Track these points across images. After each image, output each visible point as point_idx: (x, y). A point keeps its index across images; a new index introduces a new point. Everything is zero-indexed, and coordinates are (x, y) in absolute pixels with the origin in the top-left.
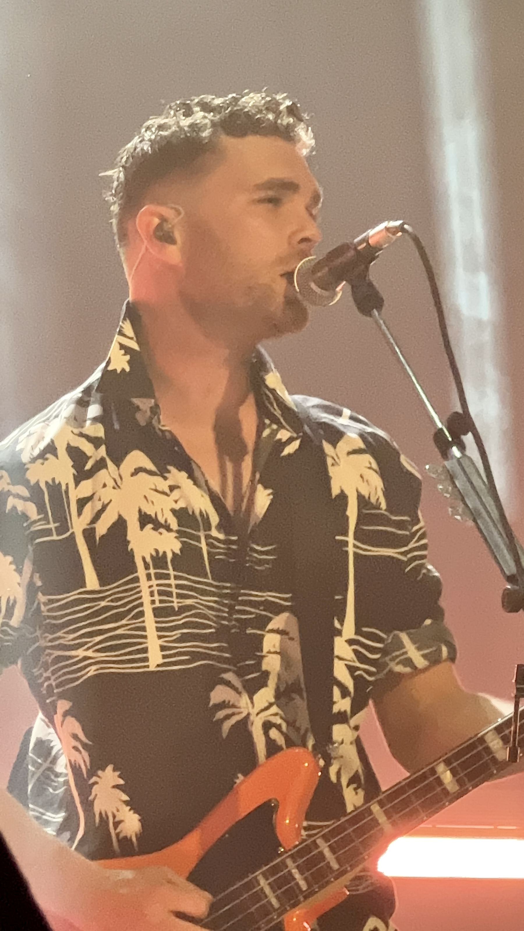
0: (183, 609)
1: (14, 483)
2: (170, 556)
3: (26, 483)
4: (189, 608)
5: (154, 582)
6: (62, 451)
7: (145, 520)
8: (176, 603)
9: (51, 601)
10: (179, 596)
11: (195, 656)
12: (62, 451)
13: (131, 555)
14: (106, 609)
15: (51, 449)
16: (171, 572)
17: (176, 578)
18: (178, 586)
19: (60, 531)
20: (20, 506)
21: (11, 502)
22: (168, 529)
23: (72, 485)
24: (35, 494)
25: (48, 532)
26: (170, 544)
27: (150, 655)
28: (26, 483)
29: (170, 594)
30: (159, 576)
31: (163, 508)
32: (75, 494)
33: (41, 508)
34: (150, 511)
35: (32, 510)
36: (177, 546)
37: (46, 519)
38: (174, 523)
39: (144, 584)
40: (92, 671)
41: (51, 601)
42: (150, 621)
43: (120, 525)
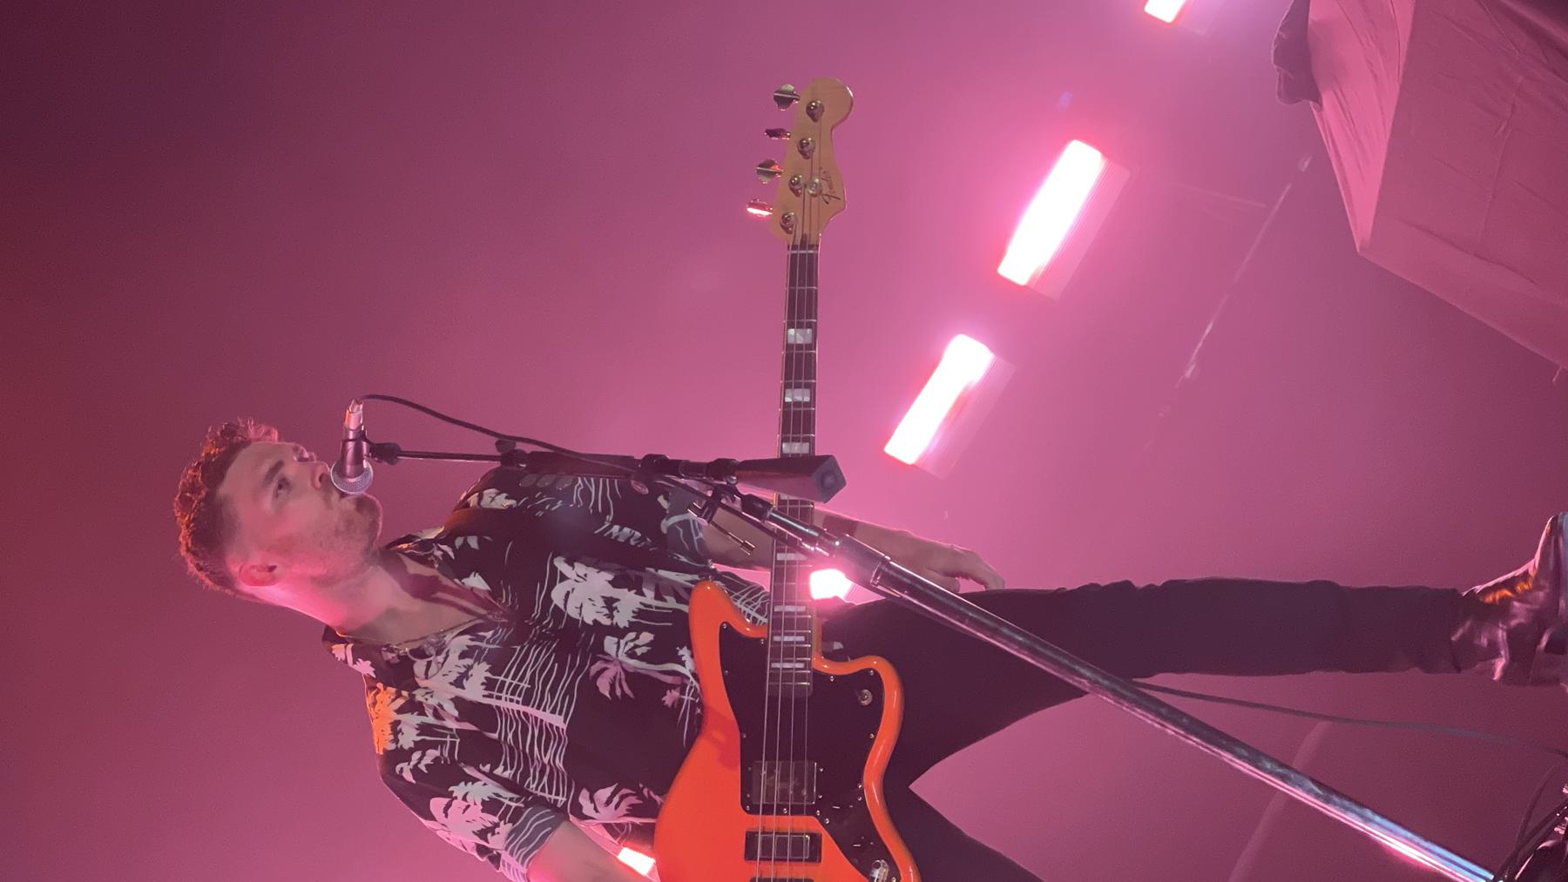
0: (532, 681)
1: (409, 760)
3: (412, 751)
4: (533, 674)
5: (503, 695)
7: (458, 683)
8: (525, 685)
10: (521, 680)
11: (569, 691)
20: (427, 760)
22: (470, 668)
23: (423, 719)
24: (421, 746)
26: (481, 671)
27: (555, 724)
28: (412, 751)
30: (500, 690)
31: (455, 665)
35: (432, 754)
38: (469, 661)
39: (503, 704)
40: (559, 764)
43: (458, 701)
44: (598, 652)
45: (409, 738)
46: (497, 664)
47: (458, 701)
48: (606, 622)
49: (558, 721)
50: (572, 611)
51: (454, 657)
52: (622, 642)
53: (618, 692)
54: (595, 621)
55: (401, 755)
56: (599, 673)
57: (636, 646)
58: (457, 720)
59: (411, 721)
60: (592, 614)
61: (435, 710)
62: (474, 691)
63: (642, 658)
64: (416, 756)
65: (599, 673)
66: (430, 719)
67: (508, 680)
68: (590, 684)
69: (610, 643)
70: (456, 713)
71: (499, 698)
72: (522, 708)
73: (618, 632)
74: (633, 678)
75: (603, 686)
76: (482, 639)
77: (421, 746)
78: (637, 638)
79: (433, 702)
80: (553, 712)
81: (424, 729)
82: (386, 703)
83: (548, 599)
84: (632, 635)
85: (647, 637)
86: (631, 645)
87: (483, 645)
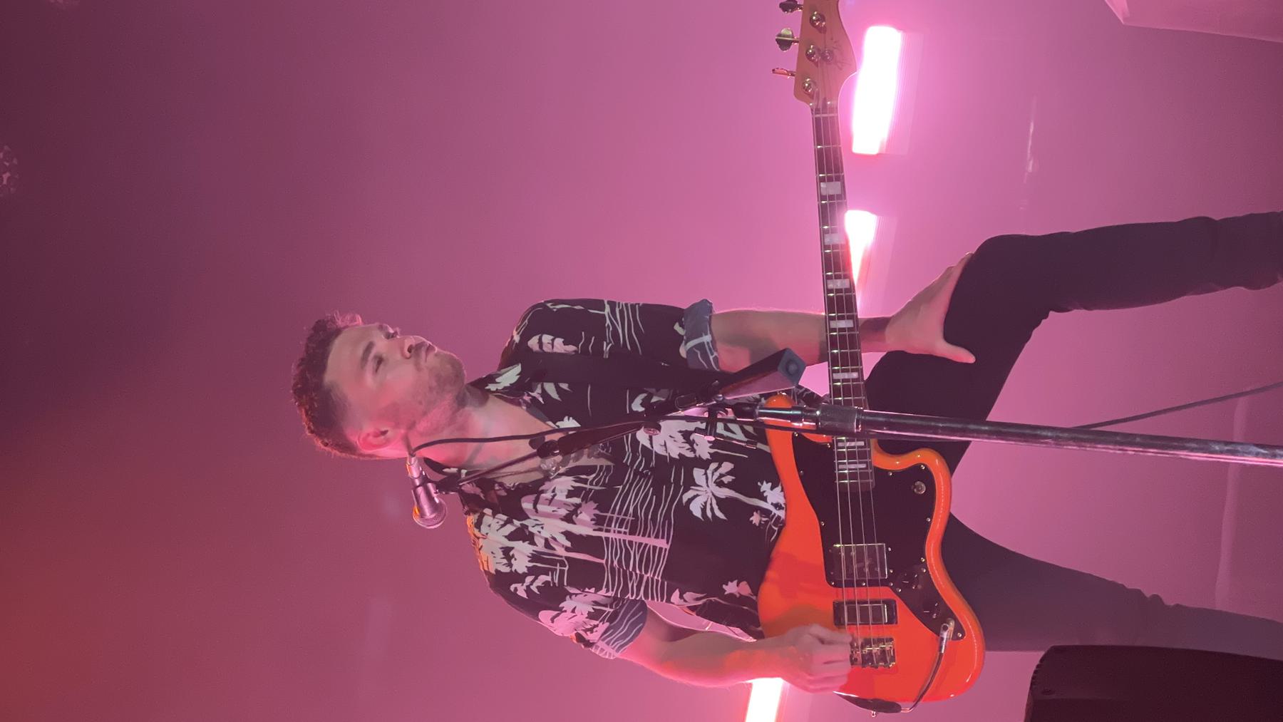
1: (523, 582)
2: (597, 512)
4: (635, 508)
6: (511, 544)
8: (630, 518)
9: (607, 586)
10: (626, 514)
11: (667, 516)
12: (511, 544)
13: (589, 537)
14: (620, 562)
15: (507, 552)
16: (609, 514)
17: (613, 512)
18: (619, 513)
19: (563, 564)
21: (534, 588)
23: (535, 548)
25: (562, 572)
28: (525, 575)
29: (623, 520)
30: (609, 525)
32: (540, 546)
33: (546, 572)
34: (563, 512)
36: (593, 505)
37: (553, 571)
38: (577, 500)
41: (607, 586)
42: (637, 539)
43: (568, 535)
44: (690, 483)
45: (521, 565)
46: (603, 500)
47: (568, 535)
48: (690, 455)
49: (662, 544)
50: (658, 449)
51: (561, 497)
52: (709, 472)
53: (709, 514)
54: (680, 455)
55: (520, 578)
56: (690, 500)
57: (722, 475)
58: (567, 549)
59: (523, 551)
60: (676, 449)
61: (546, 540)
62: (583, 526)
63: (729, 486)
64: (529, 579)
65: (690, 500)
66: (540, 546)
67: (615, 516)
68: (684, 509)
69: (698, 474)
70: (568, 544)
71: (608, 531)
72: (628, 538)
73: (704, 464)
74: (722, 503)
75: (696, 509)
76: (585, 481)
77: (533, 571)
78: (719, 466)
79: (546, 534)
80: (657, 537)
81: (535, 557)
82: (494, 531)
83: (635, 442)
84: (713, 466)
85: (727, 466)
86: (717, 474)
87: (588, 486)
